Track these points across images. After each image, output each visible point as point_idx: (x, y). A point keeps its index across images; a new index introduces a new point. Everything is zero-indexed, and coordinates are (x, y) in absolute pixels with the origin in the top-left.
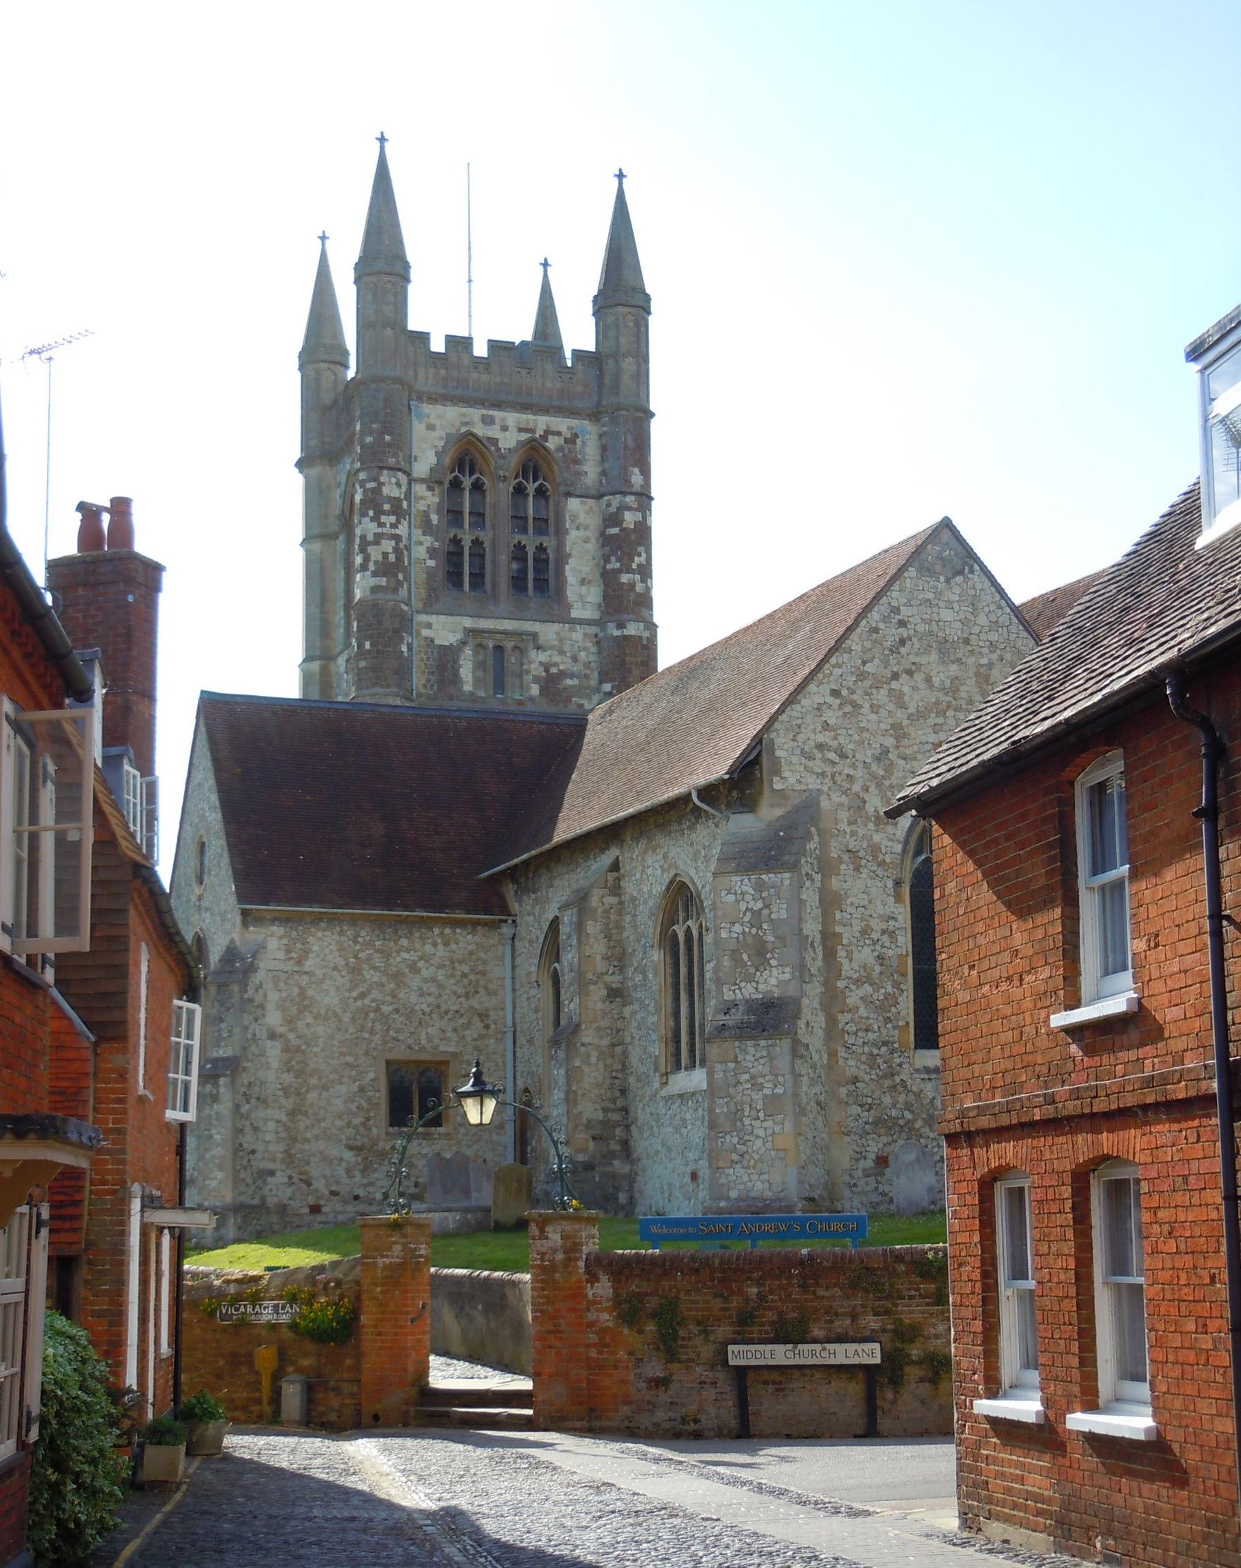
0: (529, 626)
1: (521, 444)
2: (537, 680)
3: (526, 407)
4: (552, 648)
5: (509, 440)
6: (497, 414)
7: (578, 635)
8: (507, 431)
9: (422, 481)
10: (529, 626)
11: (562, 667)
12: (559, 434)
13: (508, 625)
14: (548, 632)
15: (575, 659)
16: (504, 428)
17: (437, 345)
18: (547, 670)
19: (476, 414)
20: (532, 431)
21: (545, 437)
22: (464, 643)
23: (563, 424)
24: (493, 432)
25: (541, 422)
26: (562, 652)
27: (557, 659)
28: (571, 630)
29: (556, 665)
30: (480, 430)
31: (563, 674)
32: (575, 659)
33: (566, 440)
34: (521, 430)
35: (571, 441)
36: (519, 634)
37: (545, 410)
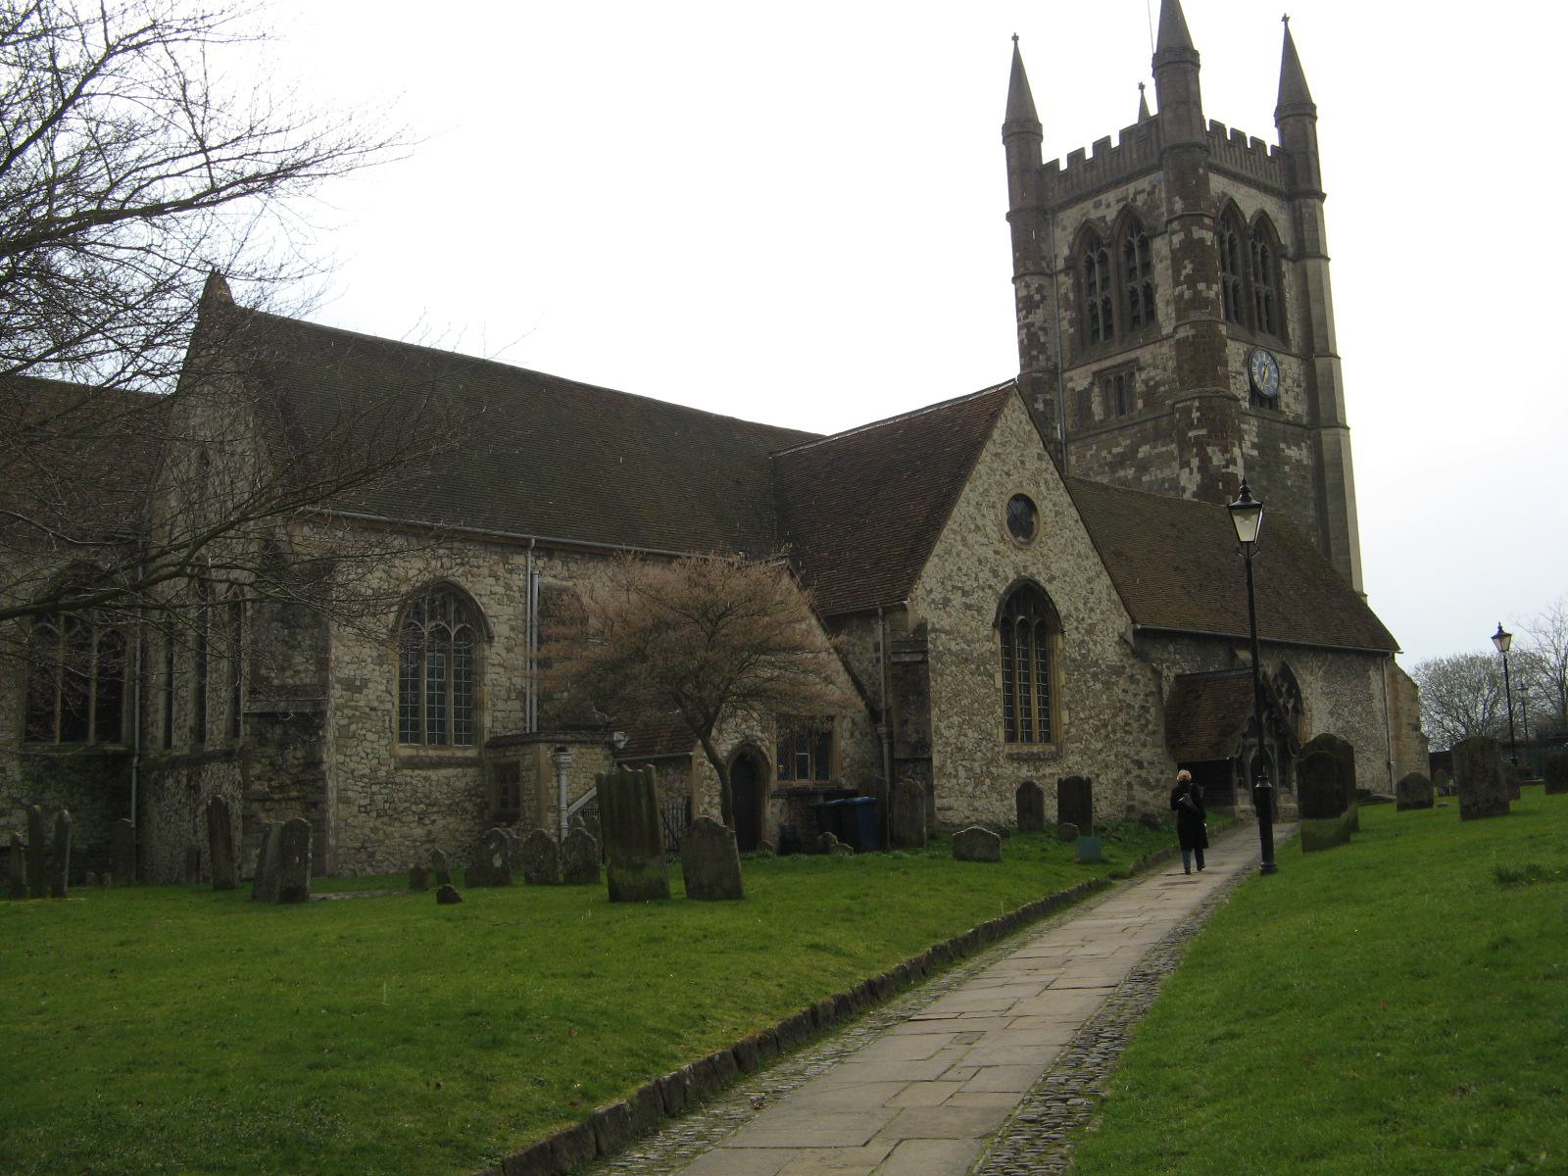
0: (1132, 355)
1: (1120, 213)
2: (1142, 395)
3: (1116, 184)
4: (1149, 366)
5: (1111, 214)
6: (1102, 197)
7: (1165, 349)
8: (1107, 209)
9: (1061, 271)
10: (1132, 355)
11: (1157, 378)
12: (1143, 191)
13: (1120, 359)
14: (1145, 354)
15: (1165, 369)
16: (1108, 206)
17: (1063, 166)
18: (1147, 385)
19: (1089, 204)
20: (1126, 198)
21: (1134, 200)
22: (1092, 384)
23: (1144, 184)
24: (1100, 213)
25: (1131, 187)
26: (1156, 367)
27: (1153, 374)
28: (1161, 346)
29: (1152, 378)
30: (1094, 215)
31: (1157, 385)
32: (1165, 369)
33: (1149, 194)
34: (1118, 201)
35: (1151, 193)
36: (1126, 363)
37: (1129, 179)
